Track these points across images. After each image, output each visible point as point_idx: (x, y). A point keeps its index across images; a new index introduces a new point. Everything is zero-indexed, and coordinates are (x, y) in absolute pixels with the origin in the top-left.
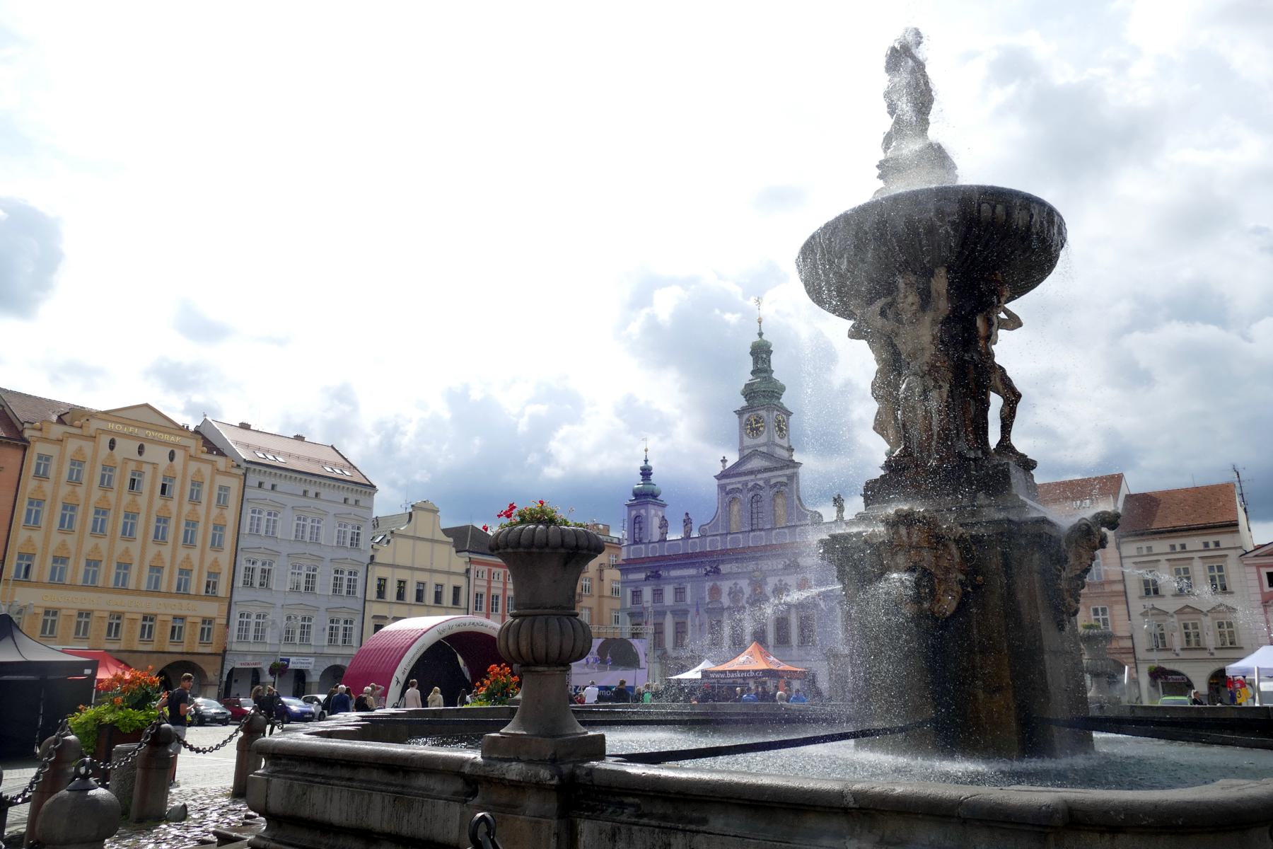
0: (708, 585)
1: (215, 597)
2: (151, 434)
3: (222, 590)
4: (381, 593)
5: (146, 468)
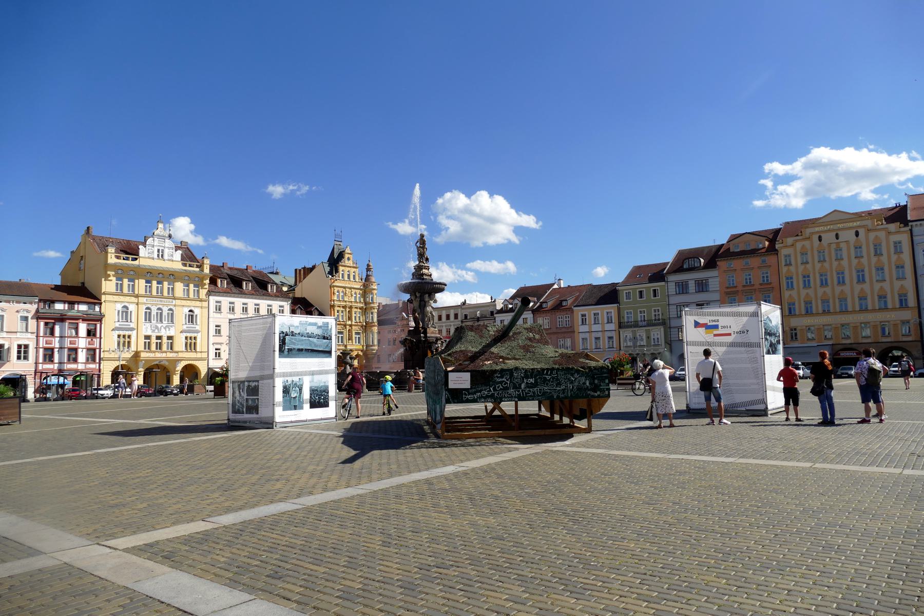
1: (907, 307)
2: (840, 226)
5: (843, 245)
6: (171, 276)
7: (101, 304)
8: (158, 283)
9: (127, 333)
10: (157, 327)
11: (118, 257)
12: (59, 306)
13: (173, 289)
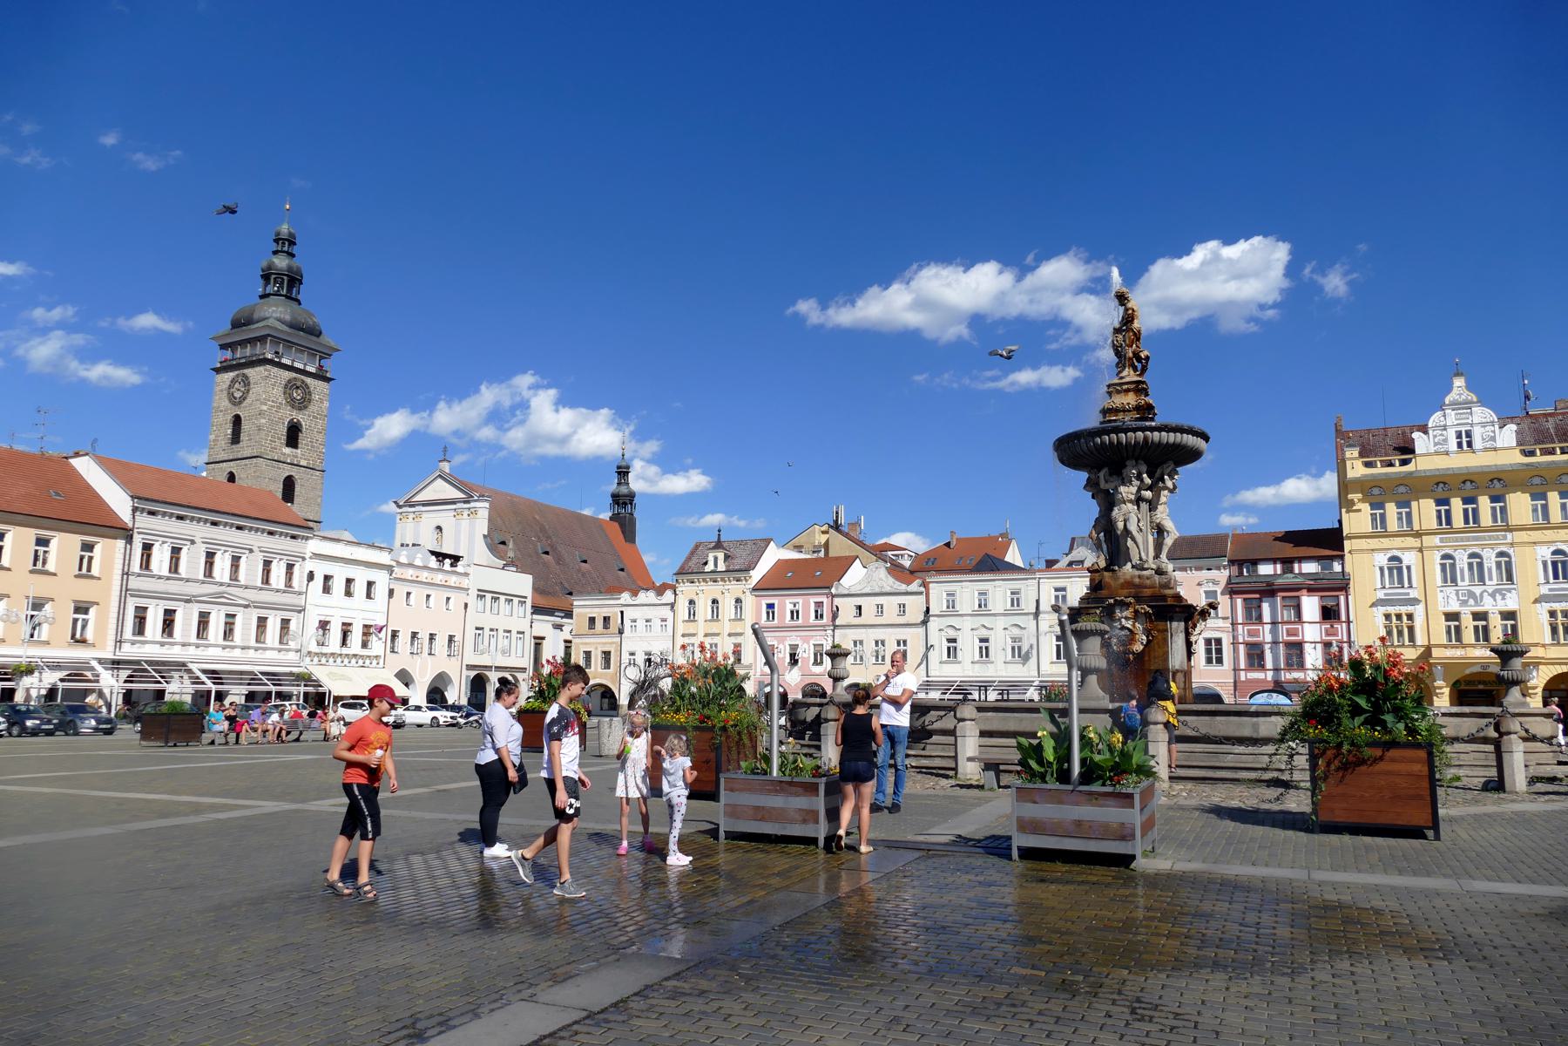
6: (1498, 484)
7: (1342, 557)
8: (1466, 501)
9: (1403, 610)
10: (1471, 595)
11: (1368, 465)
12: (1265, 569)
13: (1503, 510)
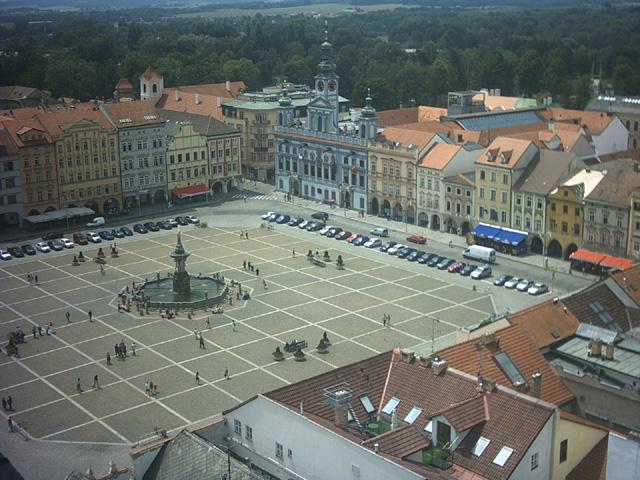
0: (304, 149)
3: (118, 174)
4: (172, 162)
